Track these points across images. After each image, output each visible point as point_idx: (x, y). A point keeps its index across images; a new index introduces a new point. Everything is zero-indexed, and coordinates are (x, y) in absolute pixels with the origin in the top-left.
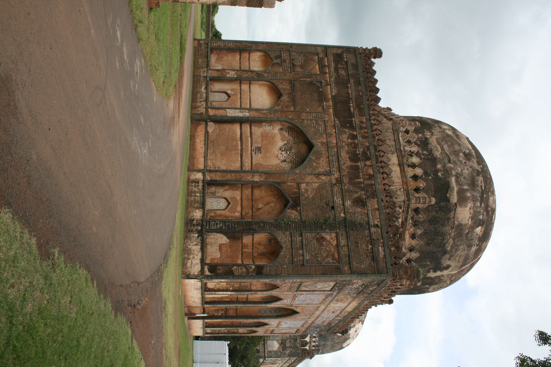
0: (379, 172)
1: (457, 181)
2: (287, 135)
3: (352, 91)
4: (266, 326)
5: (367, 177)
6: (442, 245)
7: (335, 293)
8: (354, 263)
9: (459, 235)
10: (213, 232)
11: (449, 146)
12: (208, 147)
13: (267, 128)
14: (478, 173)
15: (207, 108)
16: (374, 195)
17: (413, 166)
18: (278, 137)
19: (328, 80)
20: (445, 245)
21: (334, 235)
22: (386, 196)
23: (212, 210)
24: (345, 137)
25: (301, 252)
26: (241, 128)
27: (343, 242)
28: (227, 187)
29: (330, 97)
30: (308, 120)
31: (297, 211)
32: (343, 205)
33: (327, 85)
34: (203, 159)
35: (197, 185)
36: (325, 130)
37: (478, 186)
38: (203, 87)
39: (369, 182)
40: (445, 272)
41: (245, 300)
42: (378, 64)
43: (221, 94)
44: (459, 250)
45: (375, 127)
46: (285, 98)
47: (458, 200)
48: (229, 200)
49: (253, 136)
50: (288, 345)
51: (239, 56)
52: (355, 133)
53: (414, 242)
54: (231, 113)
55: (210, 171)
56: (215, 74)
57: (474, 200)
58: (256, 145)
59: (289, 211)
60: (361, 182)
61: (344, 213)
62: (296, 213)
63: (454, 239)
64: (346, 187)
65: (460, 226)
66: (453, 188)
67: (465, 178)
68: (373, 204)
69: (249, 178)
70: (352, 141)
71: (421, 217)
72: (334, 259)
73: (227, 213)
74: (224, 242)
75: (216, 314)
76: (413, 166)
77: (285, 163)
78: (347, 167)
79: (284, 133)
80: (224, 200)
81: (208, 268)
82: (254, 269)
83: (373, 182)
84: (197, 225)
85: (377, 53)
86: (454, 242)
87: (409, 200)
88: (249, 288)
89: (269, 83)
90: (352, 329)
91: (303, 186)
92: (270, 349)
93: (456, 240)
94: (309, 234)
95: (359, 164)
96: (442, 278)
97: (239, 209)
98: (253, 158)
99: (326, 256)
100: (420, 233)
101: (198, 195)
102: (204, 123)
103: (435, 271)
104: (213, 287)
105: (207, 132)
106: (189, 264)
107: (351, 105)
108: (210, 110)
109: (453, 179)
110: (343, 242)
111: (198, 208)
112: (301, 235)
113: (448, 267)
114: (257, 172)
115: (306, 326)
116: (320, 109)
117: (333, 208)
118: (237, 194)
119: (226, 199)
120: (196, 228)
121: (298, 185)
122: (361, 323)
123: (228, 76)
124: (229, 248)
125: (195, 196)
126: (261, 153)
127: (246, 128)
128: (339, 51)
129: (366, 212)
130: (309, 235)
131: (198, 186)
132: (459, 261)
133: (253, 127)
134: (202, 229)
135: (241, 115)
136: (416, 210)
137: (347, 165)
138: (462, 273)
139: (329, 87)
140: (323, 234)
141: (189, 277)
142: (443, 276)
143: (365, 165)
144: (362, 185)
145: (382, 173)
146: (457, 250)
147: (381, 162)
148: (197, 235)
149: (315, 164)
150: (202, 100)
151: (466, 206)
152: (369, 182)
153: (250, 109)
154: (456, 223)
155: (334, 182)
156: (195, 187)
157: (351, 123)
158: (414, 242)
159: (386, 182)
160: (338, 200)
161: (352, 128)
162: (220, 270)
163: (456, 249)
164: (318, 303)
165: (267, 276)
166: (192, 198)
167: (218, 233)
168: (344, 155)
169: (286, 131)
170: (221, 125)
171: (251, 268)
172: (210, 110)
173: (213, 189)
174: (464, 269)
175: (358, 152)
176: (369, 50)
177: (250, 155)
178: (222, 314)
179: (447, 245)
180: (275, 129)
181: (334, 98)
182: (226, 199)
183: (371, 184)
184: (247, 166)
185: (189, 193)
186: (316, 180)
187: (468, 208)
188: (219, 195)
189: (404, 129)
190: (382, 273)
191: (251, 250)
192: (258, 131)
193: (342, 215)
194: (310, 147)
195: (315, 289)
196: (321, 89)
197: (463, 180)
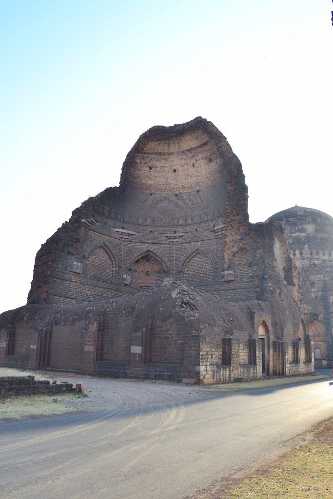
1: (294, 233)
14: (288, 221)
32: (314, 292)
53: (327, 254)
57: (304, 224)
68: (313, 278)
73: (322, 349)
87: (307, 258)
91: (306, 312)
97: (320, 343)
119: (315, 349)
136: (311, 254)
151: (306, 228)
158: (327, 254)
183: (303, 278)
187: (306, 226)
193: (320, 293)
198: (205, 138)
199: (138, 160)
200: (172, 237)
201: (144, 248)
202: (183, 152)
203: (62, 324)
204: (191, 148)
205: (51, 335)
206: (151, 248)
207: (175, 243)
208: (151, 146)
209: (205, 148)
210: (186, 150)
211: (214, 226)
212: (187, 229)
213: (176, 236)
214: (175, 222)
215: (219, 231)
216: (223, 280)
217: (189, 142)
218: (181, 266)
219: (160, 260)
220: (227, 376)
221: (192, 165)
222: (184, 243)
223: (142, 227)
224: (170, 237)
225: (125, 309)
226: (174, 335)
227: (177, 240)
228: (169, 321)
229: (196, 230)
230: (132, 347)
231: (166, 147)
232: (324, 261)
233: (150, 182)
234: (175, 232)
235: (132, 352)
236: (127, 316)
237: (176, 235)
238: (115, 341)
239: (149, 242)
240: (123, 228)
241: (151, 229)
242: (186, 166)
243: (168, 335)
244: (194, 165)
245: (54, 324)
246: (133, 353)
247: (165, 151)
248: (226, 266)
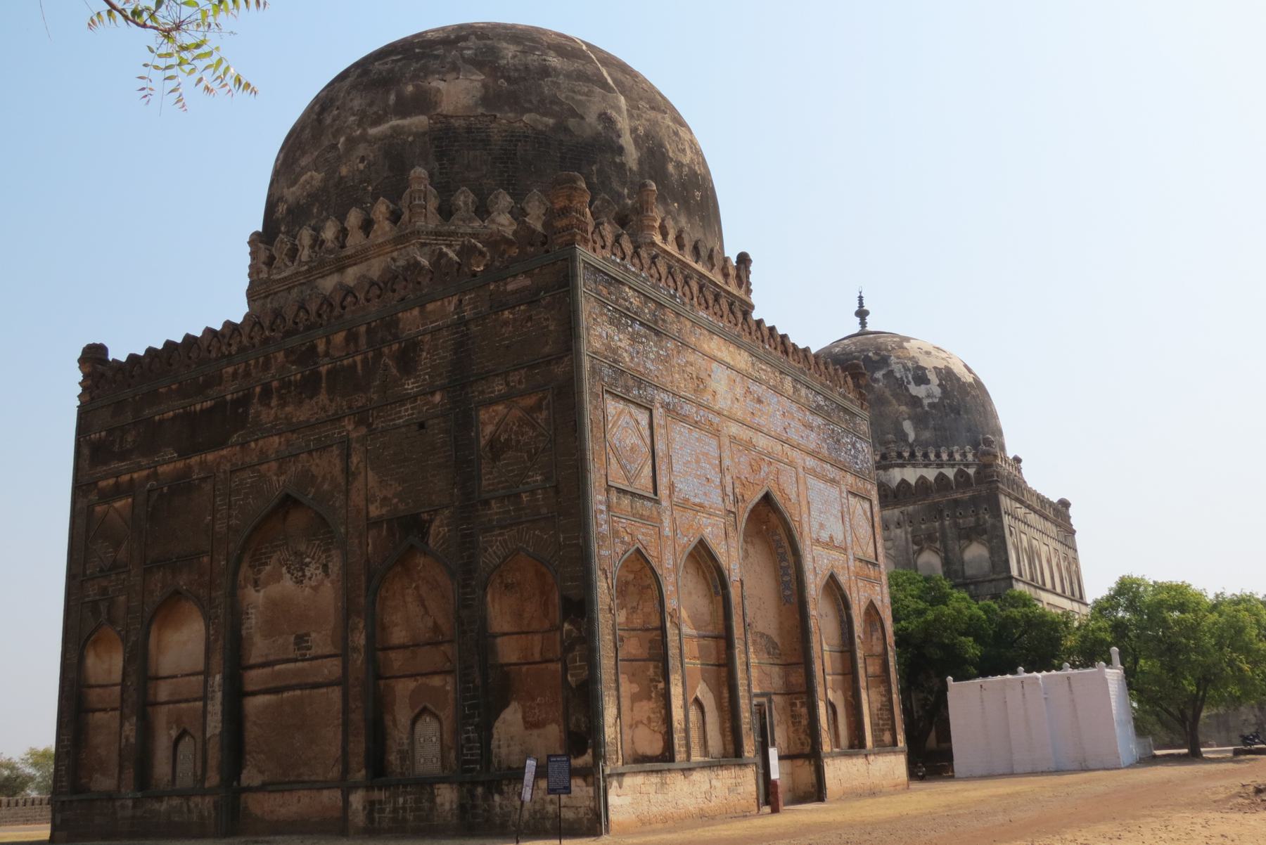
0: (341, 316)
1: (377, 121)
2: (268, 568)
3: (168, 412)
4: (842, 579)
5: (352, 345)
7: (661, 397)
8: (547, 349)
9: (514, 101)
10: (489, 751)
11: (304, 153)
12: (294, 782)
13: (253, 622)
15: (204, 793)
16: (391, 323)
17: (343, 233)
18: (274, 590)
19: (145, 473)
20: (542, 132)
22: (394, 291)
23: (443, 758)
24: (267, 415)
25: (525, 497)
26: (254, 693)
27: (499, 387)
28: (388, 719)
29: (180, 464)
30: (230, 517)
31: (431, 521)
33: (155, 473)
34: (326, 792)
35: (377, 806)
36: (251, 466)
37: (391, 71)
38: (156, 806)
39: (363, 340)
40: (623, 123)
41: (722, 643)
42: (118, 353)
43: (180, 757)
44: (555, 96)
45: (245, 340)
46: (182, 581)
47: (423, 113)
48: (417, 711)
49: (272, 658)
50: (971, 521)
51: (98, 715)
52: (258, 389)
54: (214, 724)
55: (346, 771)
56: (129, 774)
57: (426, 72)
58: (291, 647)
59: (431, 542)
60: (362, 361)
61: (433, 393)
62: (437, 522)
64: (375, 397)
65: (490, 99)
66: (394, 128)
67: (371, 104)
69: (359, 659)
70: (274, 395)
72: (538, 407)
73: (447, 714)
74: (519, 716)
75: (804, 722)
76: (343, 233)
77: (330, 565)
78: (331, 401)
79: (263, 576)
80: (419, 727)
81: (576, 757)
82: (571, 623)
83: (363, 329)
84: (473, 796)
85: (93, 357)
86: (530, 111)
88: (655, 635)
89: (154, 628)
90: (922, 364)
91: (375, 511)
92: (986, 566)
93: (527, 105)
94: (484, 483)
95: (323, 370)
96: (641, 131)
97: (436, 681)
98: (320, 652)
99: (534, 428)
100: (508, 198)
101: (401, 800)
102: (244, 796)
103: (621, 150)
104: (659, 737)
105: (263, 788)
107: (198, 407)
108: (207, 785)
109: (373, 131)
110: (499, 387)
111: (432, 799)
113: (606, 119)
114: (345, 639)
115: (832, 472)
116: (207, 487)
117: (422, 426)
118: (403, 688)
119: (414, 722)
120: (479, 802)
121: (376, 523)
122: (905, 344)
123: (132, 740)
124: (533, 699)
125: (404, 809)
126: (308, 635)
127: (254, 678)
128: (86, 451)
129: (428, 337)
131: (380, 802)
133: (252, 661)
134: (482, 784)
135: (219, 695)
136: (446, 212)
137: (327, 402)
138: (628, 81)
139: (160, 470)
140: (483, 442)
142: (634, 130)
143: (327, 354)
144: (371, 354)
145: (344, 308)
146: (555, 101)
147: (320, 316)
148: (497, 798)
149: (326, 487)
150: (185, 805)
151: (438, 90)
152: (363, 340)
153: (207, 673)
154: (480, 110)
155: (363, 430)
156: (382, 811)
157: (236, 403)
159: (361, 296)
160: (406, 413)
161: (244, 401)
163: (552, 103)
164: (714, 442)
165: (587, 585)
166: (410, 816)
167: (491, 736)
168: (303, 414)
169: (259, 572)
170: (248, 748)
171: (569, 632)
172: (207, 785)
173: (393, 758)
174: (614, 80)
175: (299, 376)
176: (86, 376)
177: (314, 663)
178: (803, 704)
179: (540, 127)
180: (256, 598)
181: (184, 454)
182: (414, 722)
183: (368, 331)
184: (332, 668)
185: (399, 829)
186: (361, 478)
187: (442, 85)
188: (406, 741)
189: (265, 268)
190: (567, 275)
191: (537, 638)
192: (259, 647)
193: (438, 398)
194: (288, 503)
195: (646, 450)
196: (165, 489)
197: (375, 109)
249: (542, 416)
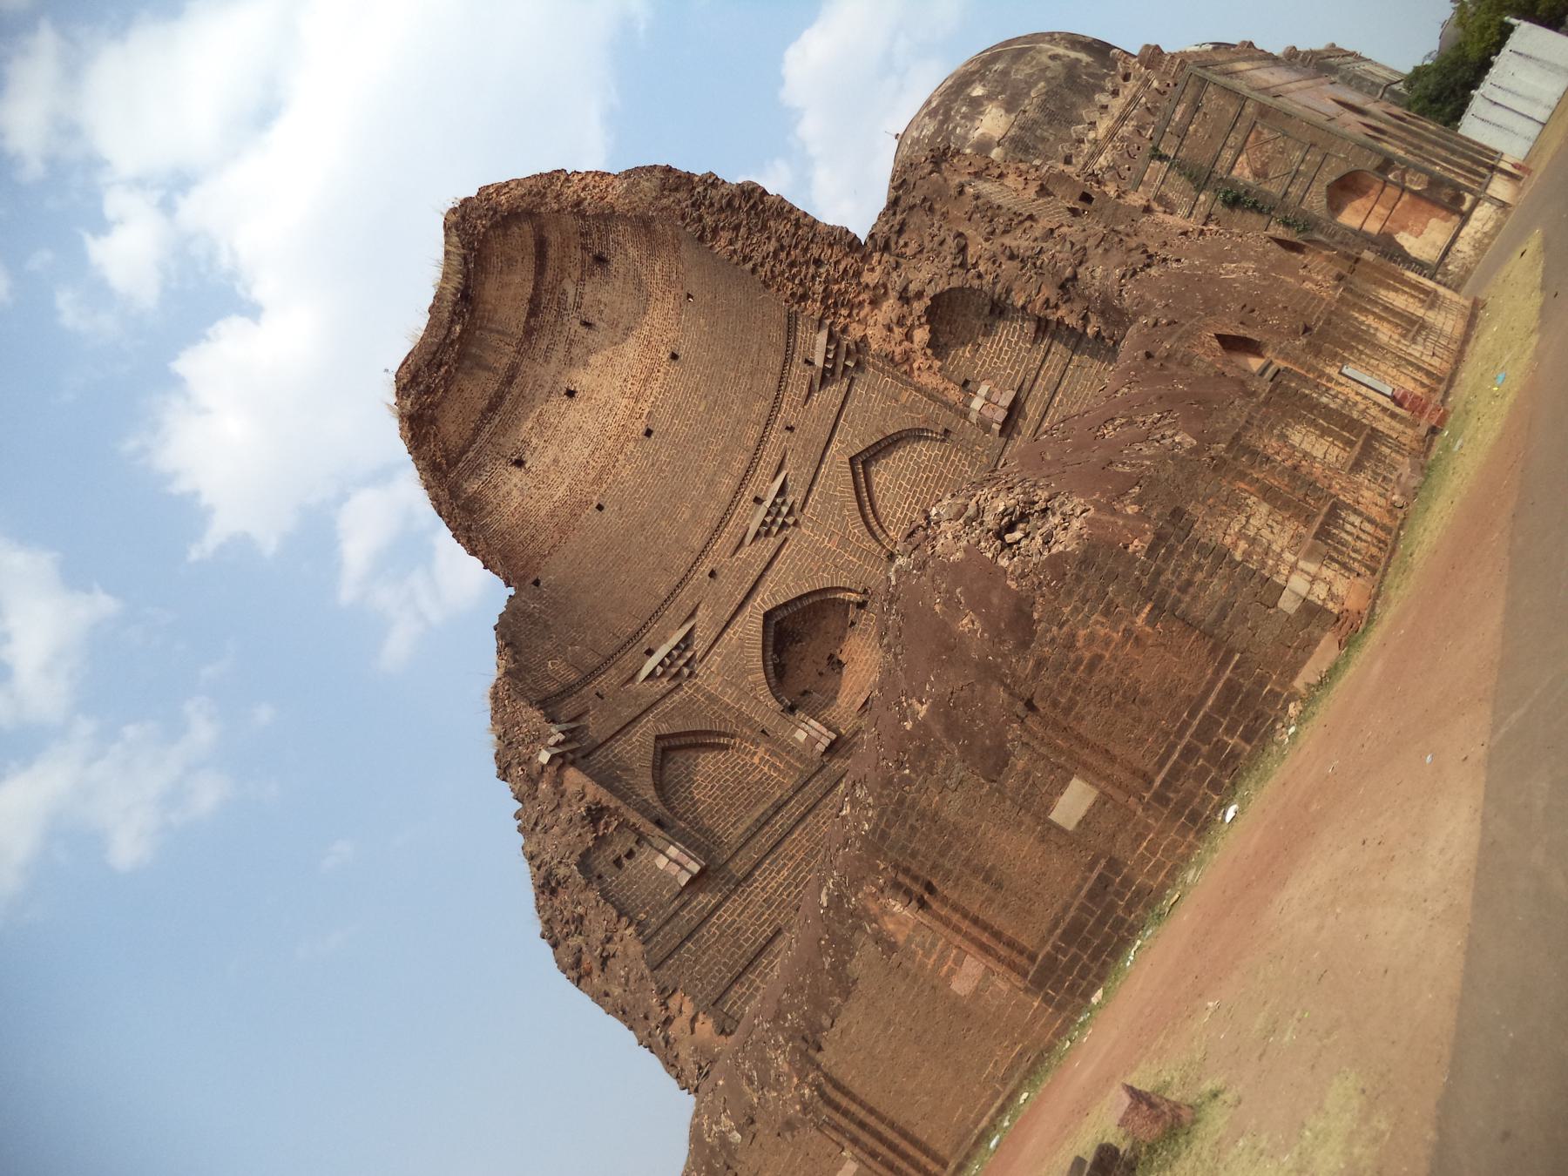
6: (1050, 94)
21: (1234, 173)
53: (1094, 115)
63: (1028, 94)
65: (1010, 107)
71: (1064, 149)
99: (1268, 142)
103: (1078, 60)
106: (1491, 224)
110: (1228, 155)
112: (1286, 193)
113: (1054, 57)
130: (1274, 188)
132: (1033, 58)
140: (1251, 180)
141: (1503, 205)
146: (1031, 75)
162: (1445, 194)
165: (1380, 152)
187: (980, 131)
193: (1202, 198)
198: (523, 234)
199: (472, 486)
200: (769, 519)
201: (750, 626)
202: (529, 332)
203: (826, 1022)
204: (531, 301)
205: (837, 1086)
206: (764, 601)
207: (790, 520)
208: (452, 426)
209: (552, 253)
210: (527, 322)
211: (809, 362)
212: (771, 456)
213: (774, 503)
214: (727, 484)
215: (836, 356)
216: (996, 427)
217: (508, 295)
218: (874, 545)
219: (817, 598)
220: (1368, 527)
221: (583, 331)
222: (809, 491)
223: (683, 594)
224: (764, 523)
225: (900, 764)
226: (1102, 632)
227: (785, 510)
228: (1040, 621)
229: (791, 429)
230: (1055, 816)
231: (483, 375)
232: (1111, 134)
233: (561, 492)
234: (758, 501)
235: (1070, 826)
236: (930, 769)
237: (768, 503)
238: (993, 867)
239: (740, 598)
240: (650, 653)
241: (705, 569)
242: (576, 351)
243: (1087, 655)
244: (587, 324)
245: (811, 1052)
246: (1079, 823)
247: (493, 387)
248: (954, 395)
249: (1266, 134)
